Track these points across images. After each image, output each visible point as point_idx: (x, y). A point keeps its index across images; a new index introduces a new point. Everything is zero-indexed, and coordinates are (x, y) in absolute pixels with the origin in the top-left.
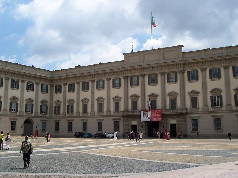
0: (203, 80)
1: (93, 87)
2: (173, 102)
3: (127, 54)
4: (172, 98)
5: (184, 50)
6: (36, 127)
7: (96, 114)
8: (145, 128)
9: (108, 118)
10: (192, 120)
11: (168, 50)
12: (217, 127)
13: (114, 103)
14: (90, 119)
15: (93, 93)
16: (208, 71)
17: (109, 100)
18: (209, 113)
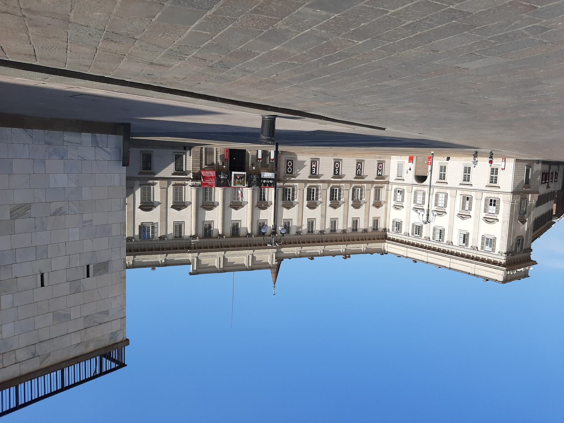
6: (410, 169)
15: (324, 216)
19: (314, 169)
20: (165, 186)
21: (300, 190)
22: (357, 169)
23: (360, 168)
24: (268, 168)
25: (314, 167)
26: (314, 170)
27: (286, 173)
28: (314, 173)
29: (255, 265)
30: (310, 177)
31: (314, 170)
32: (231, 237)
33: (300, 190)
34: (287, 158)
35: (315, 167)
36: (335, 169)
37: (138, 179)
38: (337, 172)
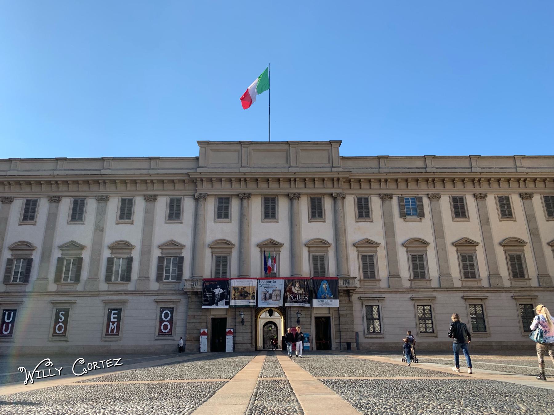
1: (101, 214)
3: (208, 143)
4: (316, 254)
5: (344, 151)
8: (249, 327)
9: (143, 298)
10: (366, 306)
11: (310, 148)
12: (428, 325)
14: (79, 301)
15: (99, 229)
16: (395, 201)
18: (403, 292)
19: (112, 320)
20: (392, 279)
21: (145, 277)
22: (13, 322)
23: (5, 325)
24: (213, 317)
25: (113, 323)
26: (114, 318)
27: (174, 309)
28: (113, 312)
29: (235, 151)
30: (124, 302)
31: (114, 318)
32: (278, 195)
33: (145, 277)
34: (172, 338)
35: (111, 323)
36: (65, 322)
37: (435, 290)
38: (60, 315)
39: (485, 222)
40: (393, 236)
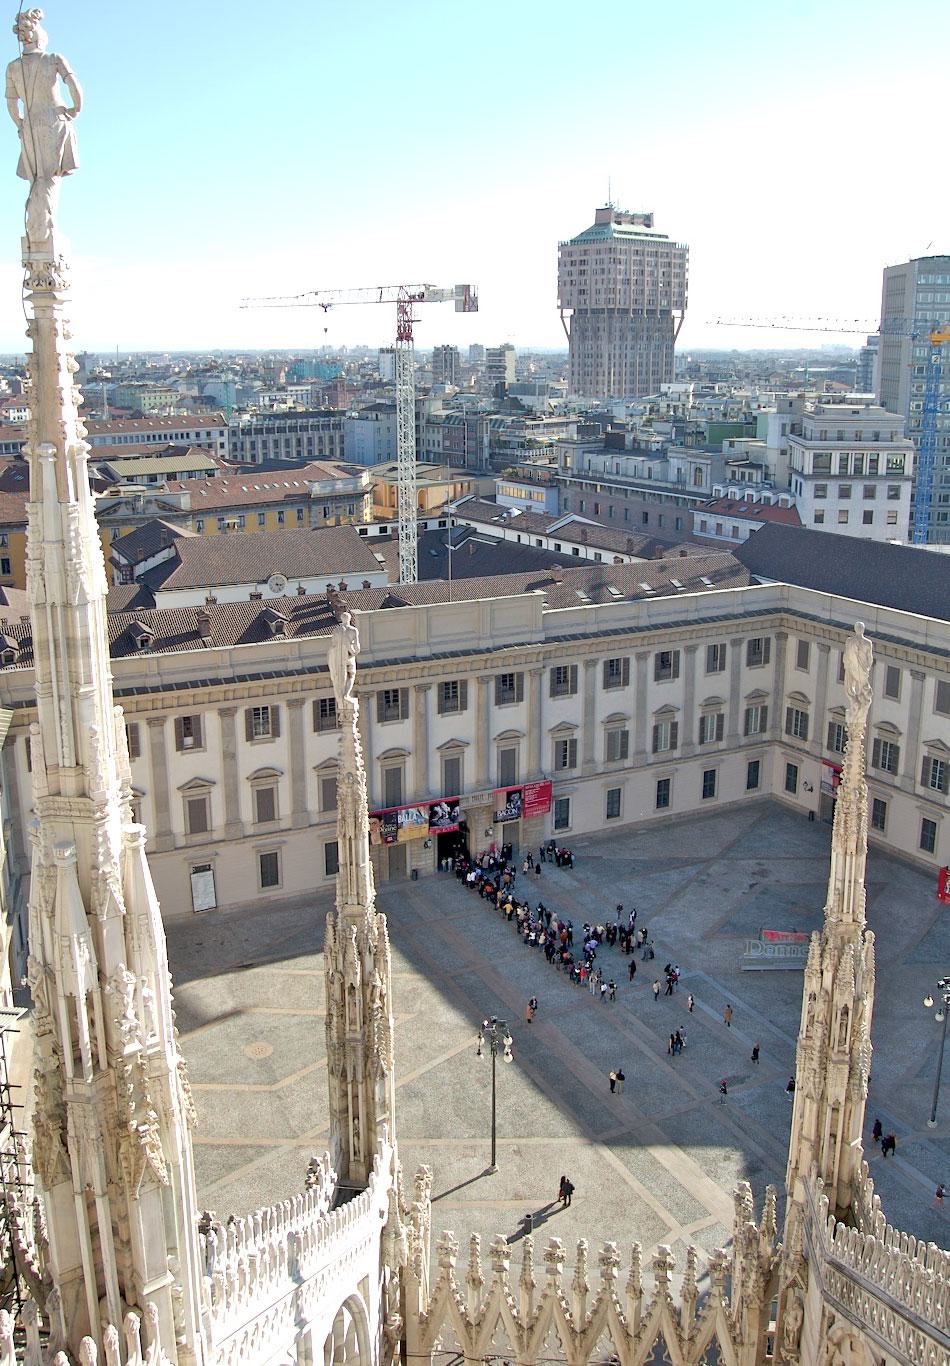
0: (586, 690)
2: (508, 759)
7: (250, 830)
13: (321, 782)
15: (230, 756)
17: (298, 778)
39: (690, 682)
40: (593, 713)
